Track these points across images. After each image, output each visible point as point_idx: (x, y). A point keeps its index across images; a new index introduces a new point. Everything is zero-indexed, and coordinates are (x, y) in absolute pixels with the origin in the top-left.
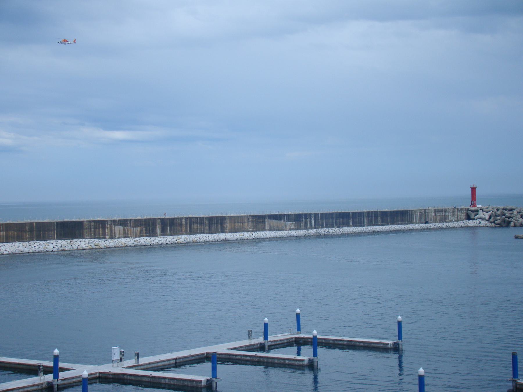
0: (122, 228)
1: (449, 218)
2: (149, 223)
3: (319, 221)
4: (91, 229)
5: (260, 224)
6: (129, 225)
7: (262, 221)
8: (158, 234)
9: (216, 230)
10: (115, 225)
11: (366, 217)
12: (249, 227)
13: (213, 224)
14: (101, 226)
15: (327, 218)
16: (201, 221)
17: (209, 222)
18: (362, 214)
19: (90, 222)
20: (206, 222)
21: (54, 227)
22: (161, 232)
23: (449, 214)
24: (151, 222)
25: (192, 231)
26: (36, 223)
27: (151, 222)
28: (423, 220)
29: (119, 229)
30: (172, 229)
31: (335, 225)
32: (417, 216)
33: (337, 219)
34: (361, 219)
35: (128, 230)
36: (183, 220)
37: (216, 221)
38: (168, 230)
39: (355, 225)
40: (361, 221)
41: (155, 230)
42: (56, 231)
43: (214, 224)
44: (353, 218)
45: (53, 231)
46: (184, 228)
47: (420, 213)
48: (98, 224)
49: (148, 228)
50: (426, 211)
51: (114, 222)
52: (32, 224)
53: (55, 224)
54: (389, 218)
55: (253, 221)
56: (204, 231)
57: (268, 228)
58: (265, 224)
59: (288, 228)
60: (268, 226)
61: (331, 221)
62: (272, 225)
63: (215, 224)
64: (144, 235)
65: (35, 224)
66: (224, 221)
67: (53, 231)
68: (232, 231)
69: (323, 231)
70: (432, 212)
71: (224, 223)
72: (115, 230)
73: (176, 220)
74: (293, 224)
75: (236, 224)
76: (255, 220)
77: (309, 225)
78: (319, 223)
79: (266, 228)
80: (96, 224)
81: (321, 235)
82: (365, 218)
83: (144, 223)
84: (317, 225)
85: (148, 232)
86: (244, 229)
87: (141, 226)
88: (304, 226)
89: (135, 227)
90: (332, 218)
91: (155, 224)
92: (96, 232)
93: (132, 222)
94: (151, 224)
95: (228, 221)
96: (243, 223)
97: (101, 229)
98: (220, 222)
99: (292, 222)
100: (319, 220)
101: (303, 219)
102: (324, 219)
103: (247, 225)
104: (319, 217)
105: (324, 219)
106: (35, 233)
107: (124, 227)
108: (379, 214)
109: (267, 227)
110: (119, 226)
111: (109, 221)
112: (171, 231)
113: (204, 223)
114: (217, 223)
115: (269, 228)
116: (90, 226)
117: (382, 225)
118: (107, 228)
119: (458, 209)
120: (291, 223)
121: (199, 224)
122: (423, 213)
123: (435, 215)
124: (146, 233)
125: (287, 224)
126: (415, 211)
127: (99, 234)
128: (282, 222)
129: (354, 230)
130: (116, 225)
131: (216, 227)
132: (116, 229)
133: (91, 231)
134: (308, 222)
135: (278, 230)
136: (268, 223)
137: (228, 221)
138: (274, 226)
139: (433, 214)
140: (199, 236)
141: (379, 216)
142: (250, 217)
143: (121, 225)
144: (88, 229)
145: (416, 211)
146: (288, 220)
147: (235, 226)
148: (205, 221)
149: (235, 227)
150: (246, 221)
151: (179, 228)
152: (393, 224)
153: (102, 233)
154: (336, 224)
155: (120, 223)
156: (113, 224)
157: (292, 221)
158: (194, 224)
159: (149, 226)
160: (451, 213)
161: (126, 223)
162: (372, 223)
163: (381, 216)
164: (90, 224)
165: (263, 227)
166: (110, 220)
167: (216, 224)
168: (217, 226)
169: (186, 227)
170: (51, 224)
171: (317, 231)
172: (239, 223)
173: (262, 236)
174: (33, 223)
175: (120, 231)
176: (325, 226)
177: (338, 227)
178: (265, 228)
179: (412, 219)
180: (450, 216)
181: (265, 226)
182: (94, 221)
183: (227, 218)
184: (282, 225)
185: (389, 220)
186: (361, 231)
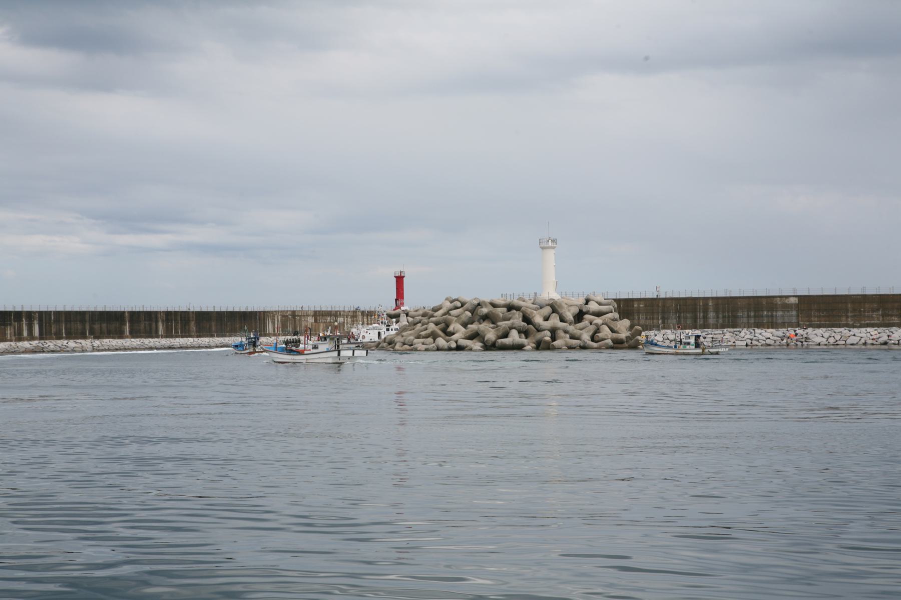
1: (344, 327)
3: (51, 326)
11: (163, 321)
15: (70, 321)
18: (153, 316)
23: (344, 320)
28: (290, 329)
31: (89, 334)
32: (276, 322)
33: (94, 324)
34: (150, 325)
39: (134, 334)
40: (151, 329)
44: (131, 321)
47: (283, 316)
50: (297, 314)
54: (213, 324)
61: (79, 326)
70: (308, 316)
77: (25, 334)
78: (51, 330)
82: (160, 324)
84: (46, 333)
88: (15, 335)
90: (83, 321)
100: (50, 323)
101: (11, 321)
102: (62, 323)
104: (51, 318)
105: (63, 322)
108: (191, 316)
117: (198, 336)
119: (363, 312)
122: (290, 317)
123: (316, 321)
126: (273, 314)
129: (125, 344)
134: (25, 328)
139: (311, 320)
141: (191, 319)
145: (274, 313)
152: (223, 336)
154: (91, 333)
160: (349, 320)
162: (176, 332)
163: (196, 320)
171: (40, 344)
176: (64, 335)
177: (97, 337)
179: (265, 326)
180: (347, 323)
185: (214, 328)
186: (142, 346)
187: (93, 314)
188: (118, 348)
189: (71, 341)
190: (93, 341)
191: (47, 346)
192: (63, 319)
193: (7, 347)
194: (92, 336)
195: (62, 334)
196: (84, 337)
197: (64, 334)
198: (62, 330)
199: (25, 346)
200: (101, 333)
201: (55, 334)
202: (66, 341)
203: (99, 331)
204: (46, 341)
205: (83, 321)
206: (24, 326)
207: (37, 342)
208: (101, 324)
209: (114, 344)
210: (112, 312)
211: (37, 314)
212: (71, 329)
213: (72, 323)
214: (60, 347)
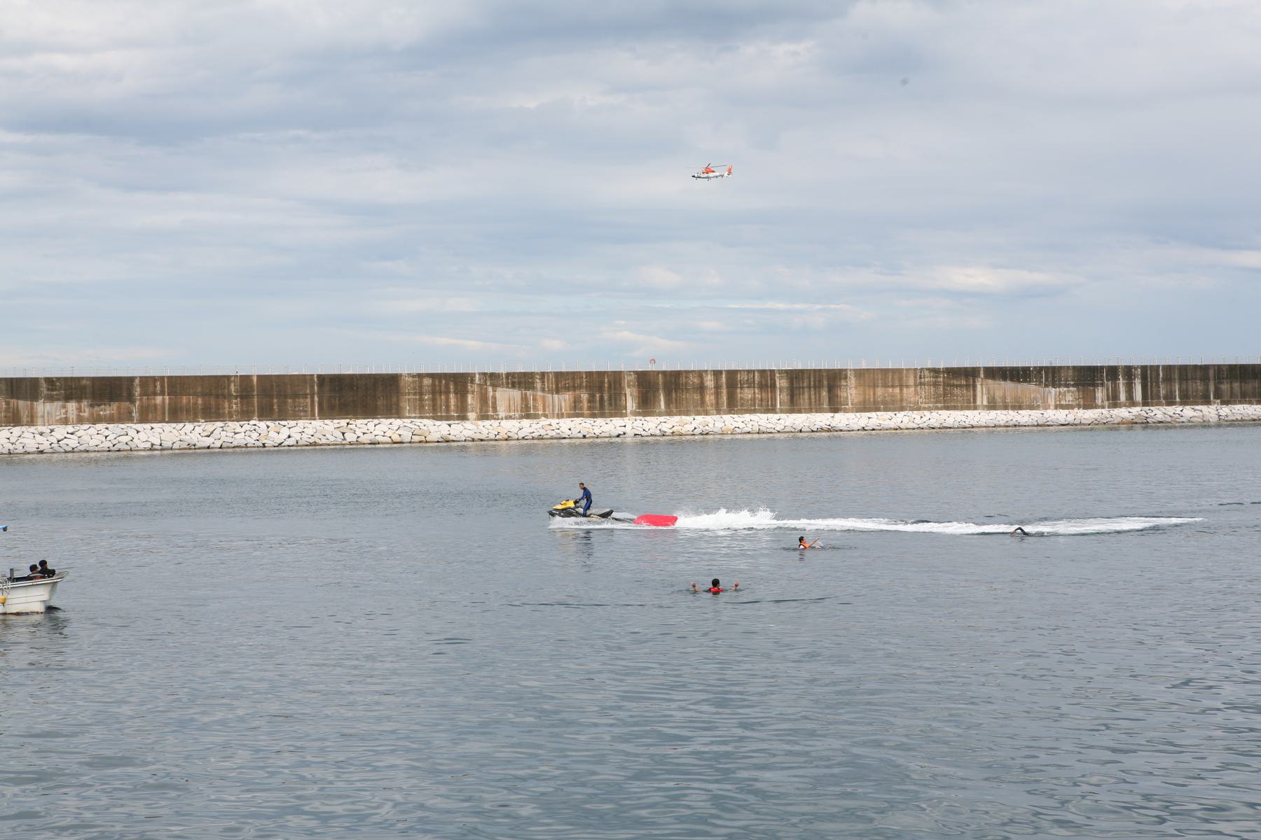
0: (516, 394)
2: (602, 383)
3: (1159, 387)
4: (421, 394)
5: (957, 391)
6: (538, 385)
7: (964, 382)
8: (629, 411)
9: (813, 403)
10: (494, 386)
12: (921, 397)
13: (803, 388)
14: (452, 387)
15: (1187, 380)
16: (766, 380)
17: (791, 383)
19: (420, 376)
20: (781, 383)
21: (312, 387)
22: (639, 407)
24: (606, 380)
25: (736, 406)
26: (258, 376)
27: (606, 380)
29: (505, 397)
30: (674, 400)
31: (1215, 398)
33: (1222, 383)
35: (535, 400)
36: (709, 376)
37: (812, 379)
38: (660, 401)
41: (620, 400)
42: (319, 397)
43: (806, 390)
45: (309, 396)
46: (710, 398)
48: (444, 382)
49: (598, 395)
51: (493, 379)
52: (246, 379)
53: (316, 379)
55: (935, 382)
56: (774, 405)
57: (985, 403)
58: (974, 390)
59: (1052, 402)
60: (985, 398)
61: (1200, 386)
62: (998, 394)
63: (810, 388)
64: (586, 412)
65: (255, 379)
66: (840, 382)
67: (309, 396)
68: (864, 407)
69: (1159, 412)
71: (840, 386)
72: (494, 398)
73: (686, 377)
74: (1070, 395)
75: (880, 391)
76: (941, 379)
77: (1123, 397)
78: (1159, 392)
79: (979, 403)
80: (437, 383)
81: (1148, 422)
83: (587, 381)
85: (598, 404)
86: (904, 405)
87: (574, 390)
88: (1108, 400)
89: (557, 392)
90: (1205, 379)
91: (620, 384)
92: (439, 403)
93: (548, 380)
94: (606, 385)
95: (852, 381)
96: (901, 386)
97: (452, 396)
98: (825, 383)
99: (1065, 389)
101: (1103, 380)
102: (1175, 382)
103: (916, 393)
104: (1159, 375)
106: (256, 400)
107: (524, 392)
109: (982, 399)
110: (508, 387)
111: (477, 376)
112: (669, 405)
113: (773, 386)
114: (818, 387)
115: (989, 402)
116: (421, 387)
118: (473, 392)
120: (1063, 389)
121: (758, 388)
124: (589, 408)
125: (1050, 392)
127: (448, 407)
128: (1032, 387)
130: (499, 386)
131: (813, 397)
132: (498, 395)
133: (421, 400)
135: (1018, 406)
136: (982, 390)
137: (853, 382)
138: (1004, 398)
140: (747, 417)
142: (927, 373)
143: (513, 386)
144: (415, 394)
146: (1053, 379)
147: (874, 394)
148: (777, 380)
149: (874, 398)
150: (911, 382)
151: (697, 397)
153: (456, 406)
154: (1218, 395)
155: (510, 381)
156: (488, 383)
157: (1067, 386)
158: (741, 388)
159: (601, 389)
161: (530, 380)
164: (421, 382)
165: (969, 400)
166: (479, 374)
167: (815, 387)
168: (815, 394)
169: (717, 394)
170: (303, 379)
172: (888, 387)
173: (949, 422)
174: (252, 376)
175: (512, 403)
176: (1178, 400)
177: (1223, 403)
178: (975, 401)
181: (975, 396)
182: (432, 376)
183: (849, 373)
184: (1032, 396)
187: (1219, 368)
188: (1256, 418)
189: (1188, 407)
190: (1219, 407)
191: (1153, 414)
192: (1177, 376)
193: (1096, 416)
194: (1219, 401)
195: (1175, 399)
196: (1207, 402)
197: (1177, 397)
198: (1175, 392)
199: (1121, 415)
200: (1231, 397)
201: (1165, 398)
202: (1181, 408)
203: (1229, 393)
204: (1151, 408)
205: (1205, 379)
206: (1121, 385)
207: (1138, 409)
208: (1231, 382)
209: (1250, 413)
210: (1249, 365)
211: (1139, 370)
212: (1187, 391)
213: (1190, 382)
214: (1170, 416)
